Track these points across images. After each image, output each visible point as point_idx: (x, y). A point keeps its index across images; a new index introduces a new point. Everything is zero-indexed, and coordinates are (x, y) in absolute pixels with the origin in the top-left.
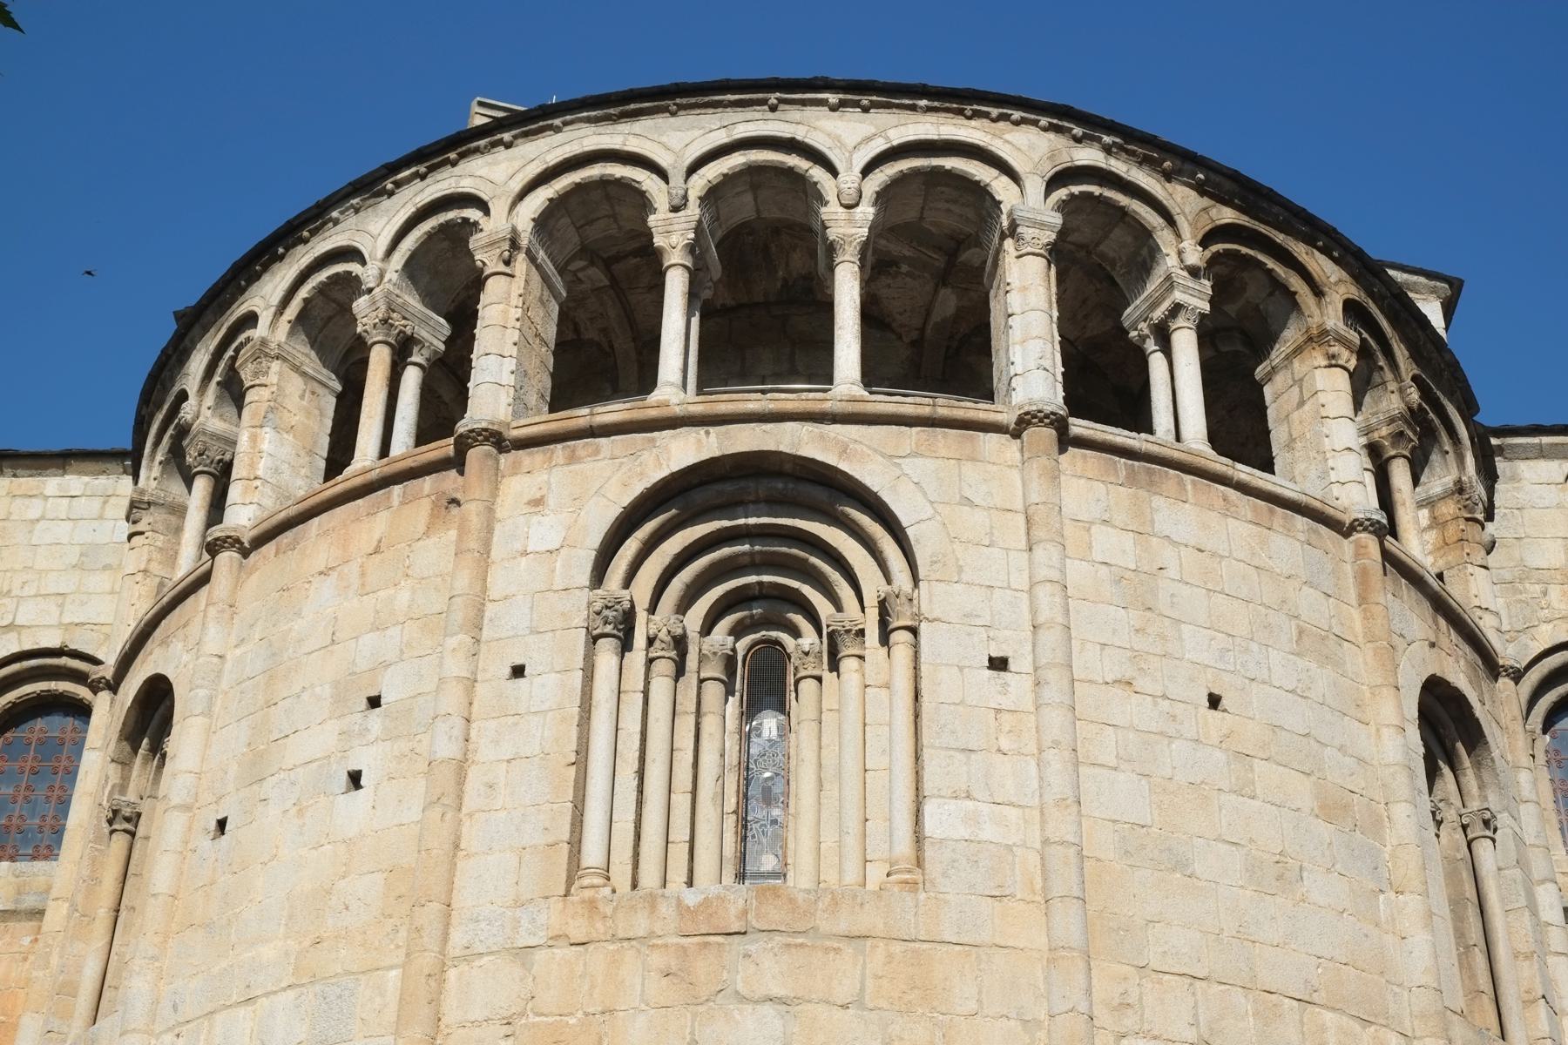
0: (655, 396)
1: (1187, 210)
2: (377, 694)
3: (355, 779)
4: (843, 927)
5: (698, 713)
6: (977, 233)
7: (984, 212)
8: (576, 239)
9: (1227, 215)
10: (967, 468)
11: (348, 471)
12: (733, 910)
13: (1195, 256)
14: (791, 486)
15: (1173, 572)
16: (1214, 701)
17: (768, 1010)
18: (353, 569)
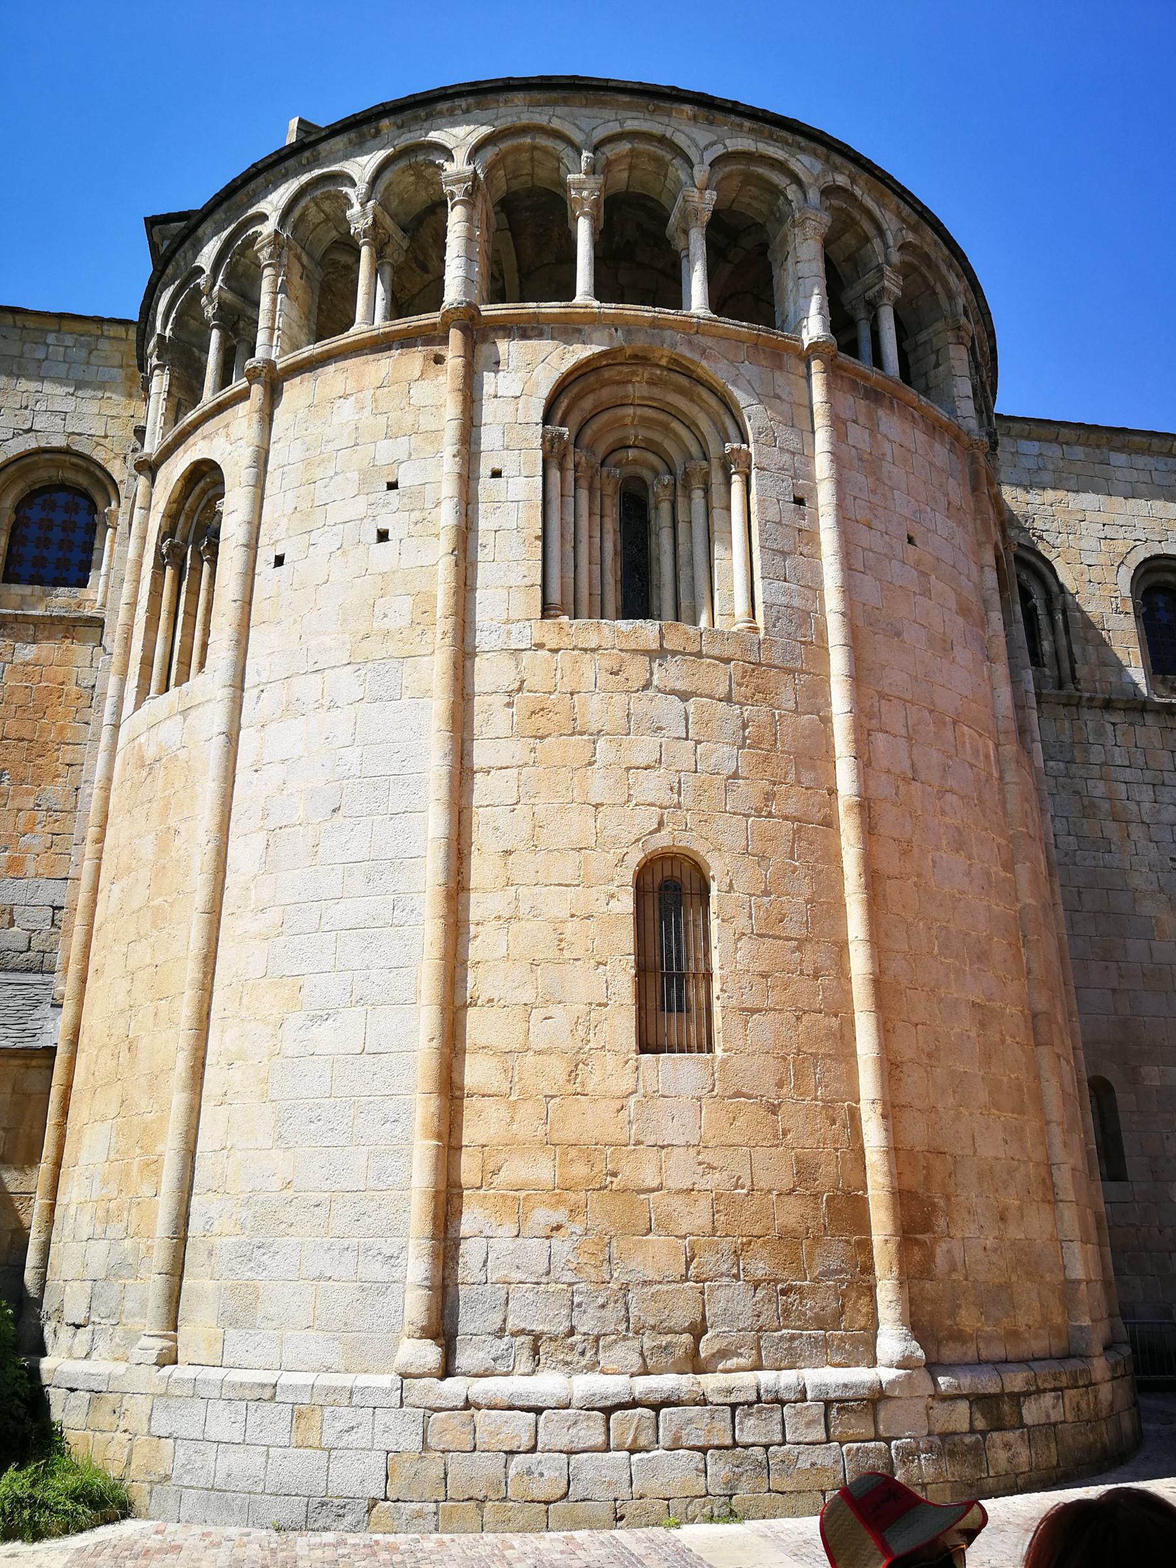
0: (574, 301)
1: (892, 228)
2: (394, 480)
3: (383, 536)
5: (602, 517)
6: (765, 223)
7: (775, 208)
8: (505, 188)
9: (910, 237)
10: (778, 374)
11: (352, 331)
13: (896, 257)
14: (665, 373)
15: (889, 458)
16: (910, 540)
18: (368, 394)
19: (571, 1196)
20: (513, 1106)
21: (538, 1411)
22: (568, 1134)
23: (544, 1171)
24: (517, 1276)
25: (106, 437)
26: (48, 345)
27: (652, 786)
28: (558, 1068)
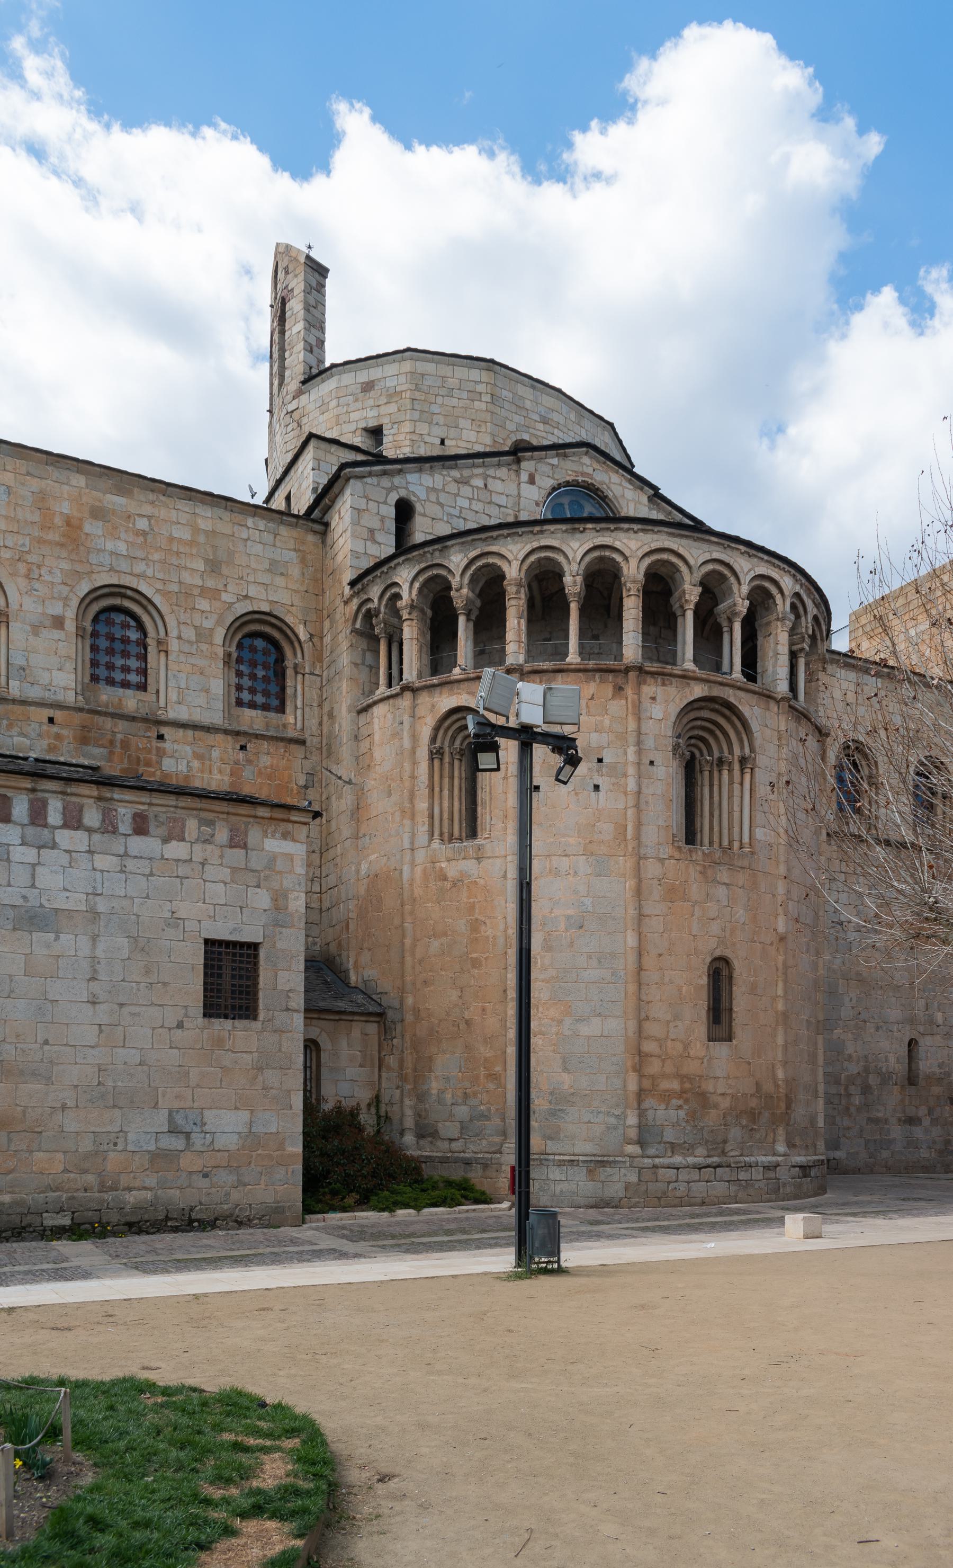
4: (740, 864)
12: (717, 856)
17: (724, 887)
19: (685, 1095)
20: (663, 1061)
21: (678, 1169)
22: (684, 1071)
23: (675, 1085)
24: (666, 1123)
25: (292, 606)
26: (248, 528)
27: (715, 928)
28: (679, 1046)
